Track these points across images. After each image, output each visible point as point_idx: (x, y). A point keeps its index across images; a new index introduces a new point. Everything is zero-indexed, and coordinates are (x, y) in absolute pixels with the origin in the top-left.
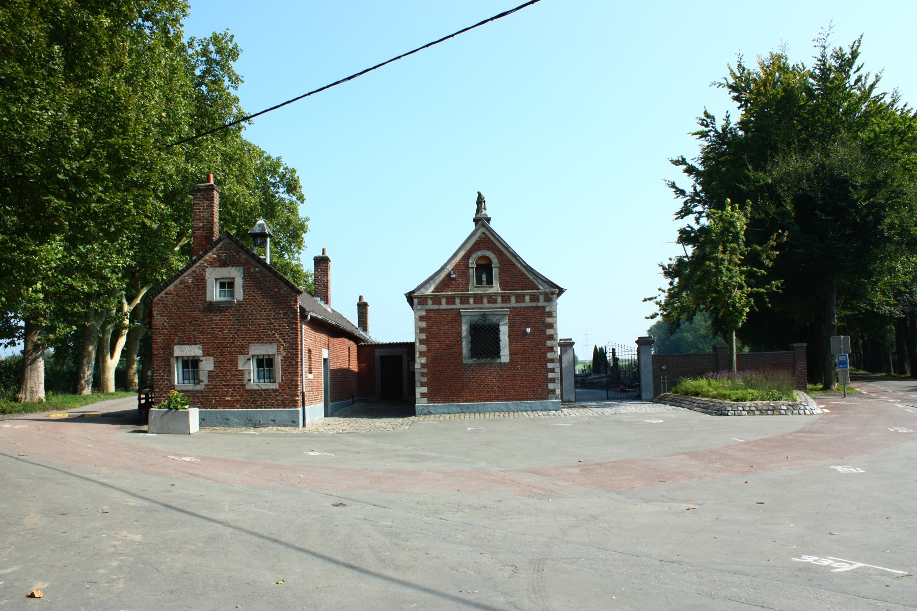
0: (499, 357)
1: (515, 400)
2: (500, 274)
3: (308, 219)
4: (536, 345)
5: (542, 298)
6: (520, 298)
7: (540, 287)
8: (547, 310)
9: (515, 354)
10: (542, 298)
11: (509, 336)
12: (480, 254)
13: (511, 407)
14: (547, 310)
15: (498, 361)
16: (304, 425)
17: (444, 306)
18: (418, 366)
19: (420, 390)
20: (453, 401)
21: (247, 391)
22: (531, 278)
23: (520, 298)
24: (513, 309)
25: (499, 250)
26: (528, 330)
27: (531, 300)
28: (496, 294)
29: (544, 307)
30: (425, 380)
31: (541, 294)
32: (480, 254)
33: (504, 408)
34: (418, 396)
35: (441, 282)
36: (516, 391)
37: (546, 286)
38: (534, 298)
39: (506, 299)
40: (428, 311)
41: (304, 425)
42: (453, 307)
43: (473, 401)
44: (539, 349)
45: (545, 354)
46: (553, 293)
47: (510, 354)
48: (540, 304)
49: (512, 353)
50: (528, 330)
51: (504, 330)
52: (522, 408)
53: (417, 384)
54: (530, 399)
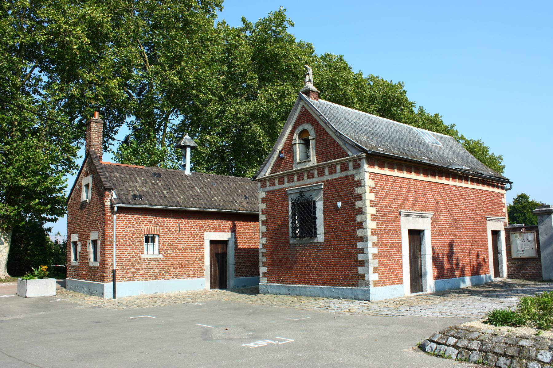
0: (316, 236)
1: (330, 284)
2: (316, 146)
3: (454, 125)
4: (347, 221)
5: (351, 164)
6: (332, 171)
7: (349, 153)
8: (356, 179)
9: (329, 233)
10: (351, 164)
11: (324, 212)
12: (300, 128)
13: (326, 292)
14: (356, 179)
15: (316, 241)
16: (114, 297)
17: (277, 187)
19: (263, 269)
20: (283, 282)
21: (89, 267)
22: (341, 144)
23: (332, 171)
24: (327, 182)
25: (315, 120)
26: (339, 204)
27: (343, 170)
28: (313, 168)
29: (353, 176)
30: (265, 260)
31: (350, 160)
32: (300, 128)
33: (320, 292)
35: (275, 164)
36: (330, 275)
37: (354, 150)
38: (345, 168)
39: (321, 173)
40: (267, 192)
41: (114, 297)
42: (283, 186)
43: (296, 283)
44: (350, 226)
45: (355, 231)
46: (360, 158)
47: (325, 233)
48: (349, 173)
49: (327, 232)
50: (339, 204)
51: (320, 205)
52: (335, 295)
53: (261, 264)
54: (342, 285)
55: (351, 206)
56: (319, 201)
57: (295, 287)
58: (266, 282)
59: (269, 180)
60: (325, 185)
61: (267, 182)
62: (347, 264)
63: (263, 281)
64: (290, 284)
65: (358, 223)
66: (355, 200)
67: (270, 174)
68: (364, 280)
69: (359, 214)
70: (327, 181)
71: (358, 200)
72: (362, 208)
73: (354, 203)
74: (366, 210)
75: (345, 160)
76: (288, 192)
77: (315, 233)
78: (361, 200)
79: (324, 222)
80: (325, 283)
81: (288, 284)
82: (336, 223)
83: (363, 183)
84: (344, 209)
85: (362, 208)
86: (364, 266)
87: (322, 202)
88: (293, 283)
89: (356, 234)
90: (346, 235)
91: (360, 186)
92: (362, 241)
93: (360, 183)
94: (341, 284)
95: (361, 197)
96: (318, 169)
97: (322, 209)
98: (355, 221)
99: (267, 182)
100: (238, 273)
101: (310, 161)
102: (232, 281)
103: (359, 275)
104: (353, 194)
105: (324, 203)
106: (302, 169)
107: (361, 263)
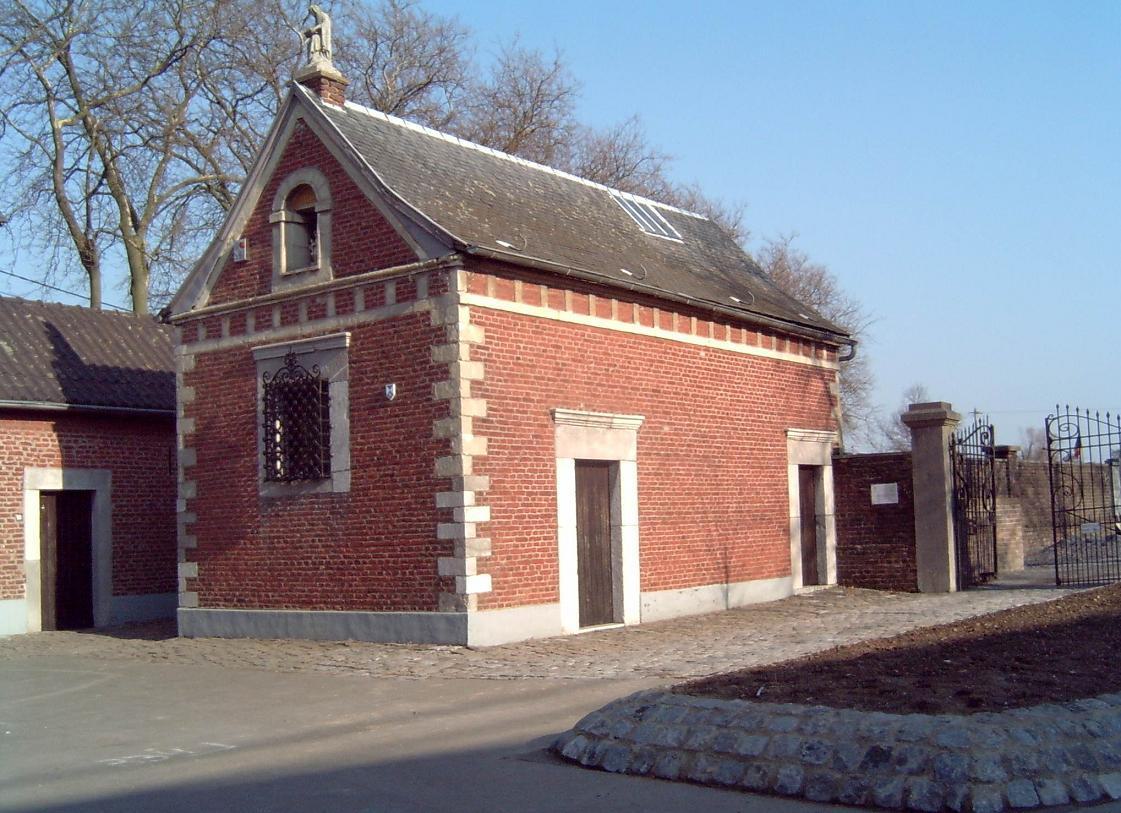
0: (329, 477)
1: (363, 605)
5: (423, 284)
7: (420, 253)
9: (364, 467)
10: (423, 284)
14: (435, 321)
17: (228, 342)
18: (181, 507)
19: (187, 570)
24: (358, 330)
25: (334, 162)
26: (392, 390)
28: (323, 291)
30: (193, 543)
34: (182, 585)
43: (276, 604)
44: (417, 449)
45: (429, 462)
47: (353, 468)
49: (358, 465)
50: (392, 390)
51: (339, 394)
53: (181, 553)
55: (424, 394)
56: (339, 379)
57: (273, 615)
58: (196, 603)
59: (204, 322)
60: (354, 339)
61: (200, 325)
62: (410, 550)
63: (188, 603)
64: (261, 607)
65: (439, 441)
66: (432, 380)
67: (209, 305)
68: (453, 591)
69: (441, 417)
70: (359, 327)
71: (440, 380)
72: (448, 401)
73: (429, 386)
74: (458, 405)
75: (409, 270)
76: (257, 357)
77: (327, 468)
78: (446, 379)
79: (351, 439)
80: (353, 603)
81: (253, 607)
82: (381, 442)
83: (454, 333)
84: (404, 404)
85: (448, 401)
86: (453, 555)
87: (346, 384)
88: (267, 604)
89: (432, 471)
90: (407, 474)
91: (446, 342)
92: (449, 489)
93: (445, 335)
94: (394, 603)
95: (447, 372)
96: (338, 294)
97: (347, 403)
98: (431, 435)
99: (200, 325)
100: (121, 586)
101: (317, 270)
102: (105, 602)
103: (441, 579)
104: (428, 362)
105: (350, 386)
106: (297, 293)
107: (445, 548)
